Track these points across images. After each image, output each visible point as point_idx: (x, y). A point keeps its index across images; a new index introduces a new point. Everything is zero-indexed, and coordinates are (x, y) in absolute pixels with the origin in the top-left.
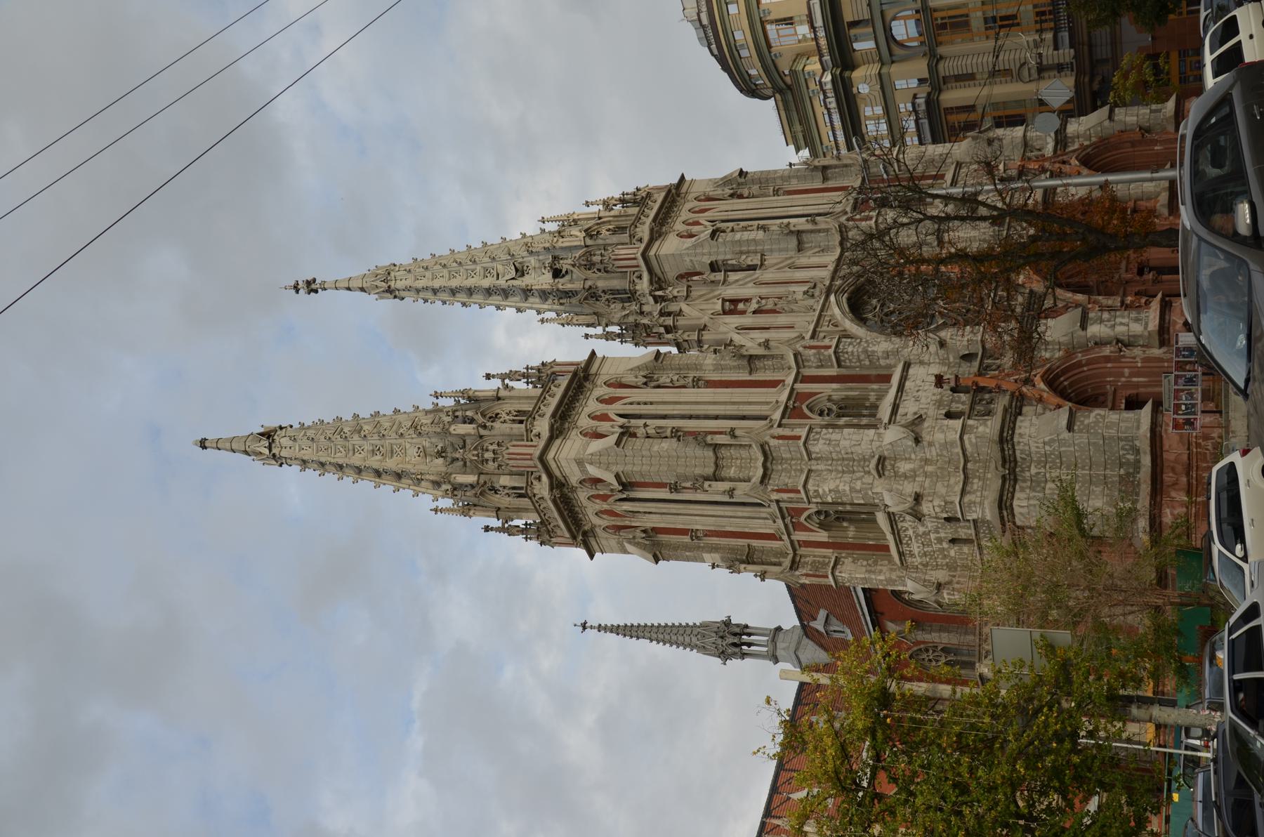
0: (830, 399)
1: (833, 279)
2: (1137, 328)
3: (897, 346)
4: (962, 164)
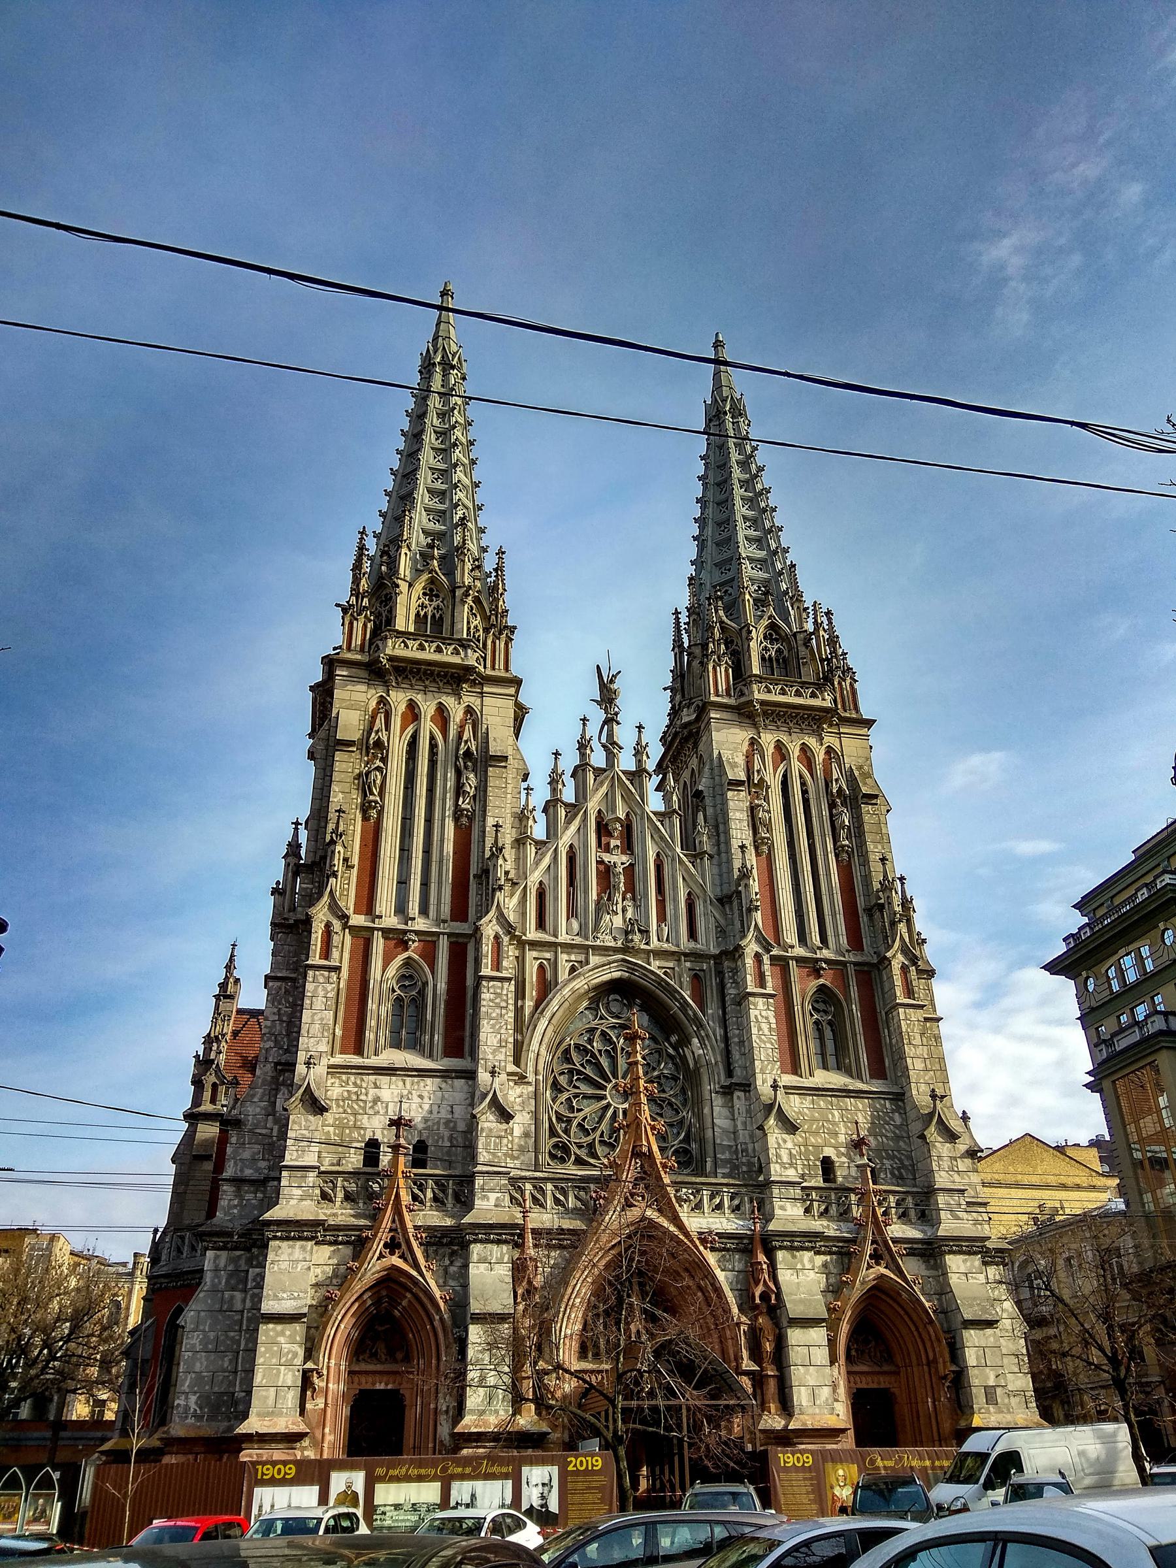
0: (425, 984)
1: (660, 954)
2: (474, 1399)
3: (490, 1057)
4: (903, 1101)
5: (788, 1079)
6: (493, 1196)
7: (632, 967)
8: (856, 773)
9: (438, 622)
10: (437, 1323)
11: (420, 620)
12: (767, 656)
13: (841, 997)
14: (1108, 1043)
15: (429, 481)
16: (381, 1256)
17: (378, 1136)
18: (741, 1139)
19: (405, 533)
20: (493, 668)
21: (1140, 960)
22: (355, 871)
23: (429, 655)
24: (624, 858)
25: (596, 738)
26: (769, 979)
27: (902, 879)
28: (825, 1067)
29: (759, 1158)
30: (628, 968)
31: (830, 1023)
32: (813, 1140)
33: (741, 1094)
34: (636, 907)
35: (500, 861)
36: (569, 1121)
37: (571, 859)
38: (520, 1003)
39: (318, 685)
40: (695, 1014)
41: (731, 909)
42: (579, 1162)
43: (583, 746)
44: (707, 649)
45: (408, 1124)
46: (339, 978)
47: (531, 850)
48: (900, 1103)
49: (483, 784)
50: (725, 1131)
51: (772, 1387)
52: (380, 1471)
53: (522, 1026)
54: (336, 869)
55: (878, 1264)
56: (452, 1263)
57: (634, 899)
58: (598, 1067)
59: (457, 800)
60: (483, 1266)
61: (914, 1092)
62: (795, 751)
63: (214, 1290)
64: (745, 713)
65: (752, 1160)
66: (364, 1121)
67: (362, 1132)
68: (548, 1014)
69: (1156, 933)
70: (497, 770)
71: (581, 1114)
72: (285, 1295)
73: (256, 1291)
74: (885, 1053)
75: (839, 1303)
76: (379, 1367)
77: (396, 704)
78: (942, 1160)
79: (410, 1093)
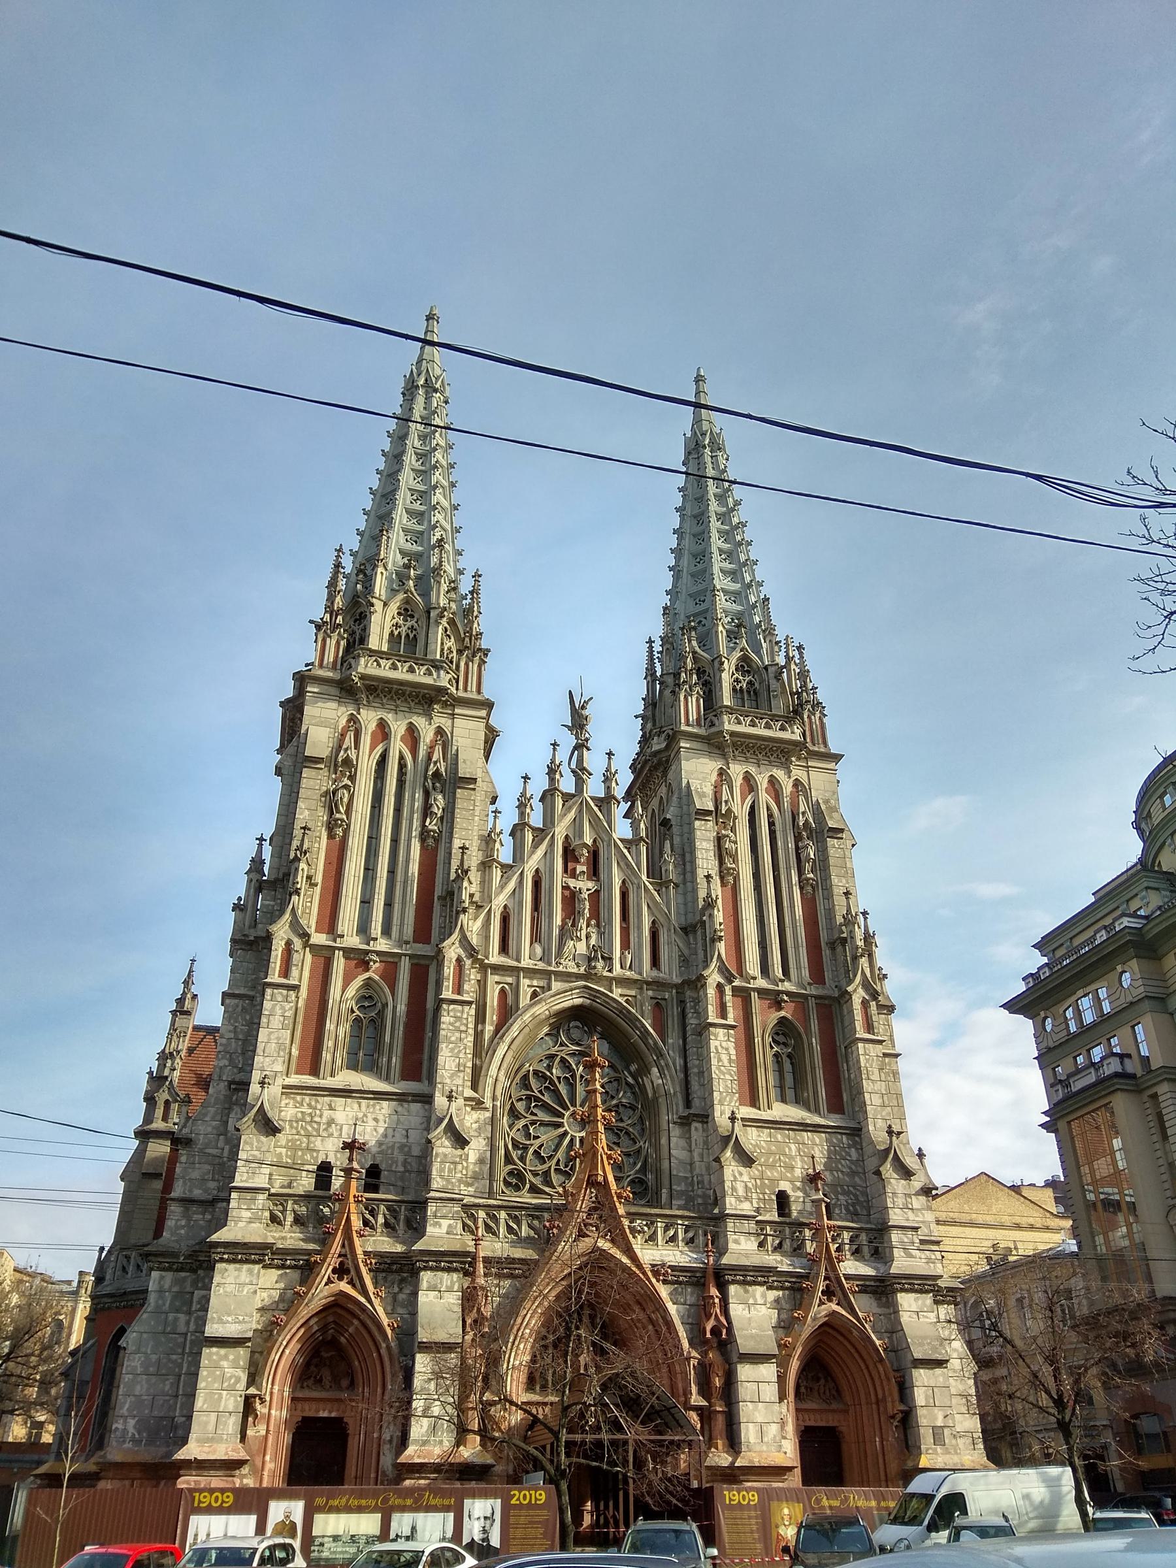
0: (385, 1005)
1: (623, 982)
2: (419, 1429)
3: (448, 1081)
4: (859, 1136)
5: (746, 1112)
6: (445, 1223)
7: (593, 994)
8: (823, 807)
9: (412, 642)
10: (383, 1351)
11: (394, 639)
12: (738, 687)
13: (802, 1030)
14: (1065, 1083)
15: (408, 502)
16: (329, 1281)
17: (331, 1159)
18: (697, 1171)
19: (382, 553)
20: (465, 690)
21: (1098, 1001)
22: (318, 889)
23: (401, 674)
24: (590, 885)
25: (565, 763)
26: (730, 1010)
27: (865, 913)
28: (784, 1100)
29: (715, 1191)
30: (590, 995)
31: (789, 1056)
32: (769, 1173)
33: (699, 1125)
34: (601, 934)
35: (465, 884)
36: (525, 1148)
37: (537, 884)
38: (480, 1027)
39: (288, 701)
40: (656, 1043)
41: (695, 939)
42: (534, 1190)
43: (552, 771)
44: (679, 679)
45: (362, 1147)
46: (297, 997)
47: (497, 874)
48: (857, 1139)
49: (450, 805)
50: (681, 1162)
51: (720, 1423)
52: (319, 1501)
53: (481, 1051)
54: (299, 886)
55: (830, 1300)
56: (401, 1289)
57: (598, 925)
58: (556, 1093)
59: (424, 821)
60: (432, 1294)
61: (871, 1128)
62: (762, 782)
63: (158, 1311)
64: (715, 744)
65: (708, 1192)
66: (318, 1143)
67: (315, 1154)
68: (508, 1039)
69: (1113, 976)
70: (466, 792)
71: (537, 1142)
72: (230, 1319)
73: (200, 1313)
74: (843, 1087)
75: (790, 1339)
76: (324, 1395)
77: (366, 722)
78: (897, 1197)
79: (365, 1115)
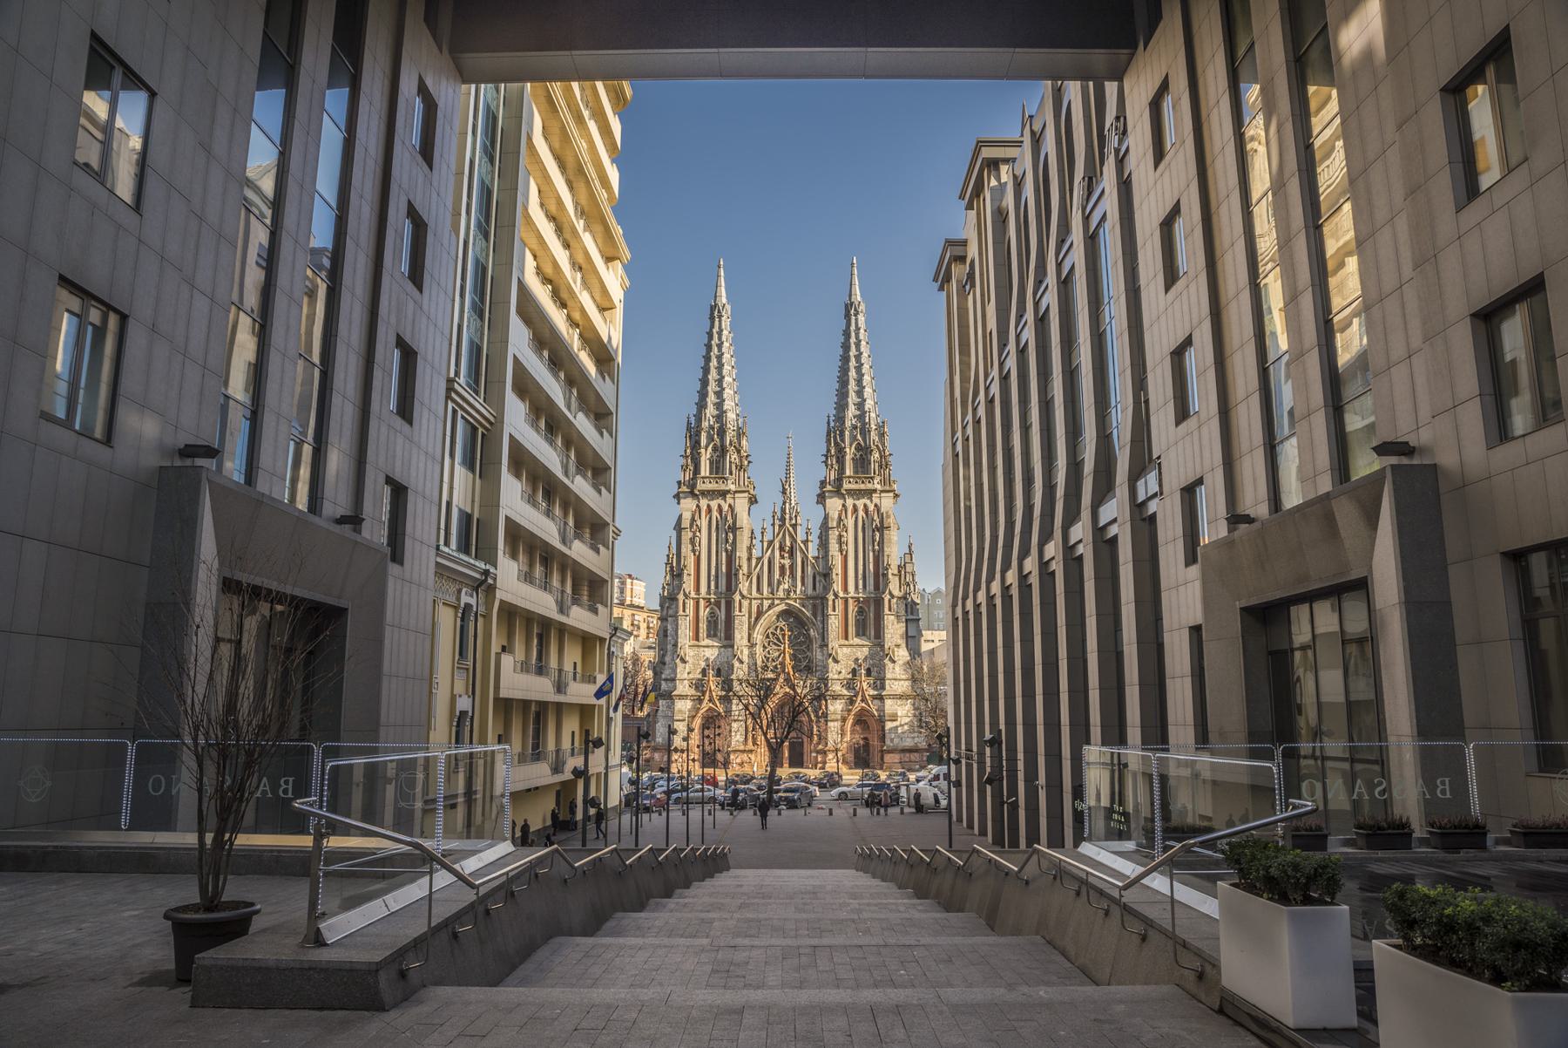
37: (770, 562)
53: (751, 628)
58: (778, 639)
62: (861, 508)
68: (759, 624)
